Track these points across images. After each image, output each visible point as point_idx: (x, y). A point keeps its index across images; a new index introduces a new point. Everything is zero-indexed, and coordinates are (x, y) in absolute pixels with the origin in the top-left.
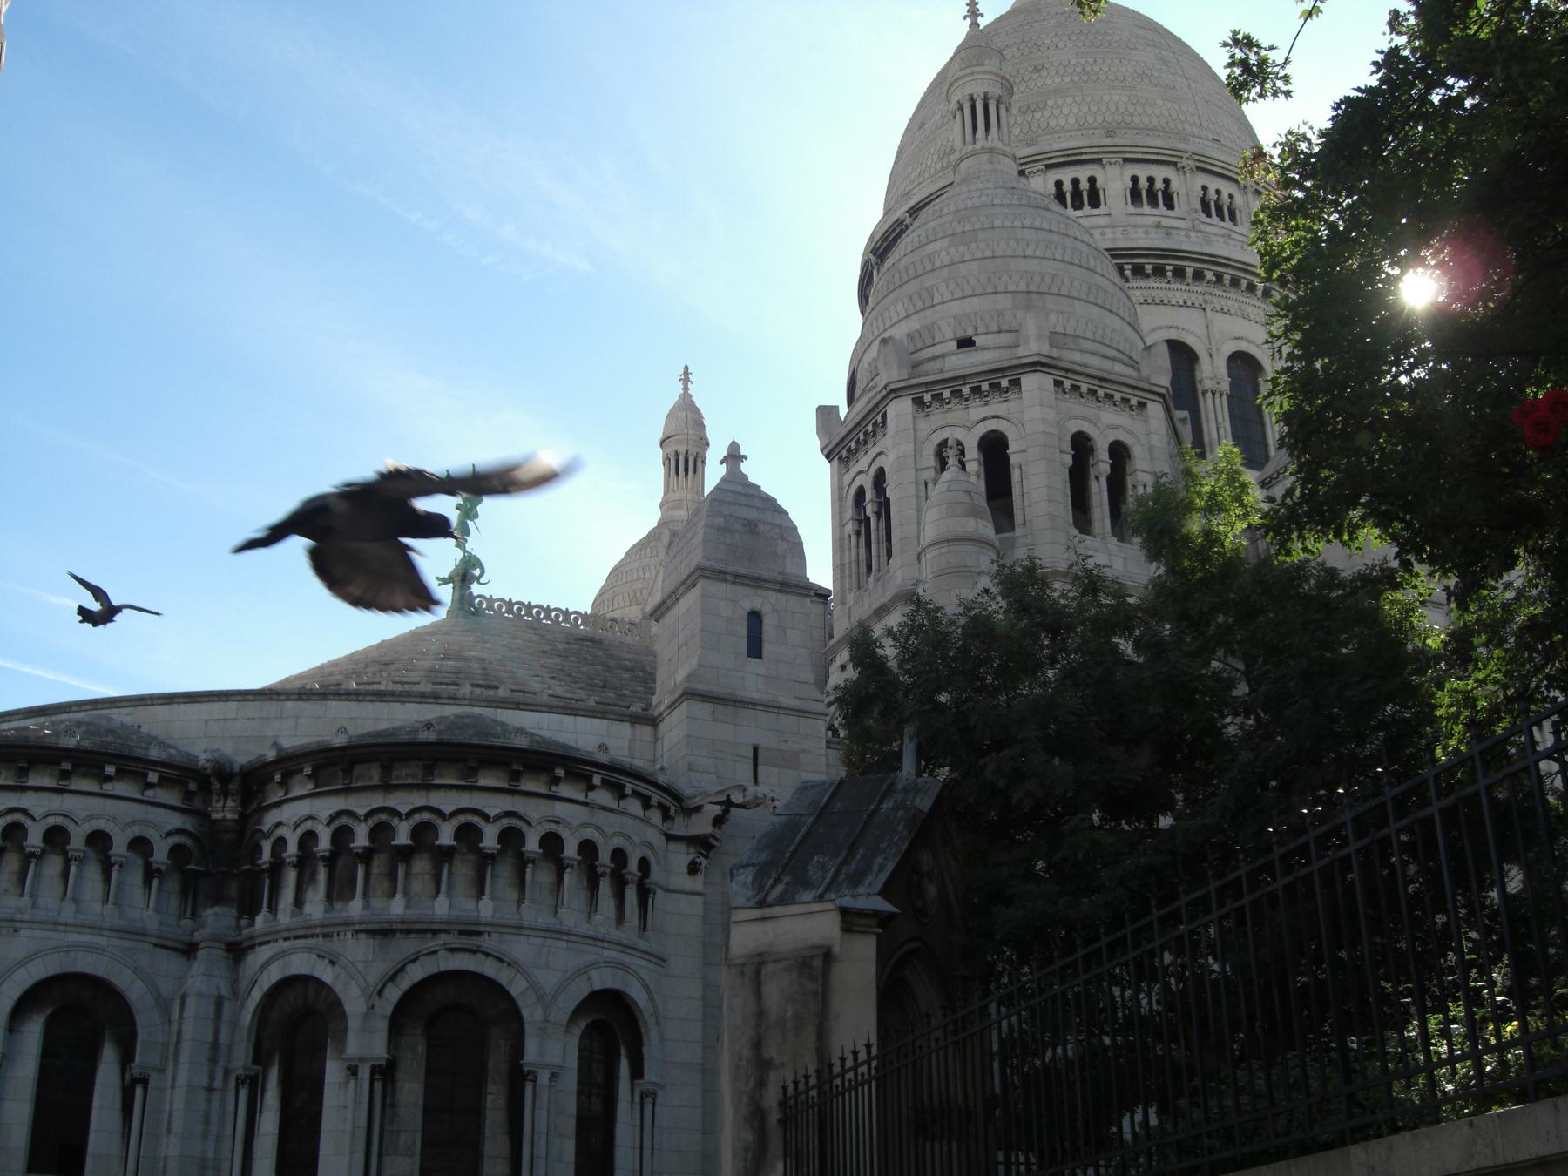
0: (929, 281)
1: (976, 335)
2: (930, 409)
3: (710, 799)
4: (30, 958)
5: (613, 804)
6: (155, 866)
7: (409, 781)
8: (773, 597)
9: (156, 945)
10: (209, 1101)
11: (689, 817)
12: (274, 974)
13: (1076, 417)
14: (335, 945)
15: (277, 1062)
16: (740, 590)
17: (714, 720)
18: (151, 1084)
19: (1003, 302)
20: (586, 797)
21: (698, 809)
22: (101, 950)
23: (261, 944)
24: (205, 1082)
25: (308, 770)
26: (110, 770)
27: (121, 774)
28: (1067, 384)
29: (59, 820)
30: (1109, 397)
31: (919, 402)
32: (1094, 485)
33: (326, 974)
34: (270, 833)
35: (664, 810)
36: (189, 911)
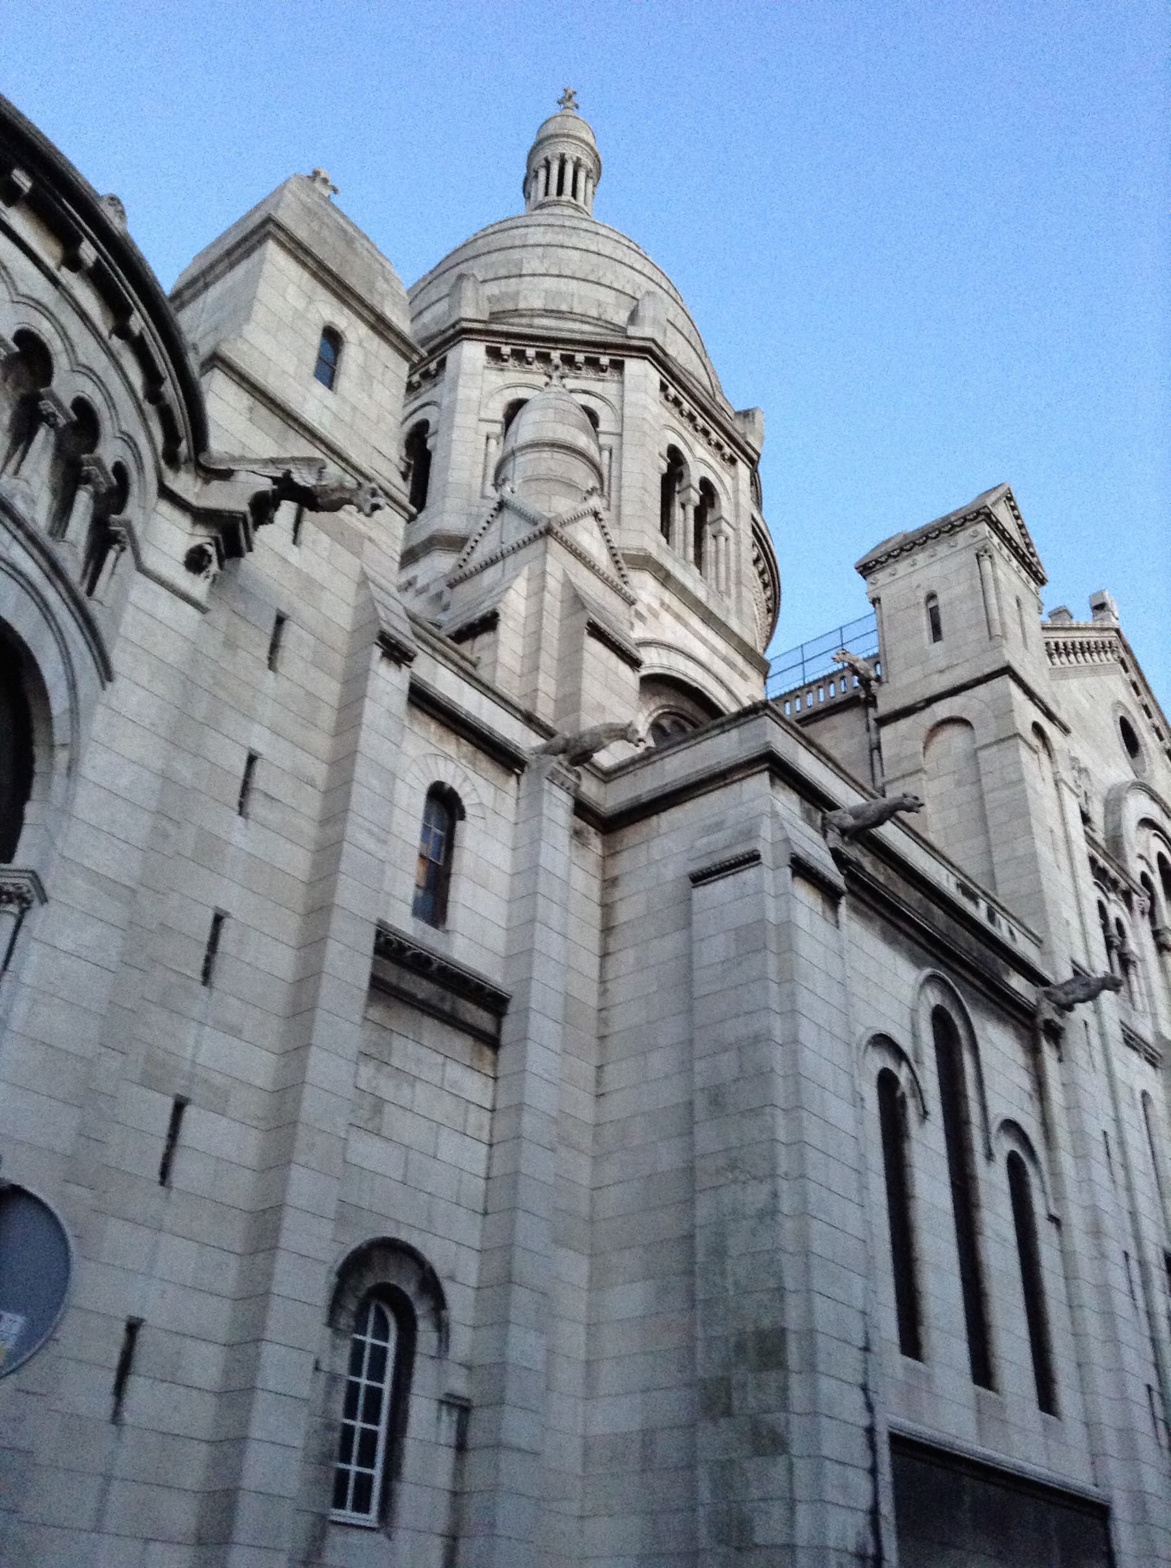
0: (516, 254)
1: (571, 313)
2: (505, 364)
3: (255, 467)
5: (105, 333)
8: (363, 330)
11: (207, 482)
13: (673, 430)
16: (322, 294)
17: (250, 420)
19: (608, 296)
20: (59, 269)
21: (226, 475)
28: (672, 391)
30: (706, 433)
31: (494, 354)
32: (678, 513)
35: (172, 438)
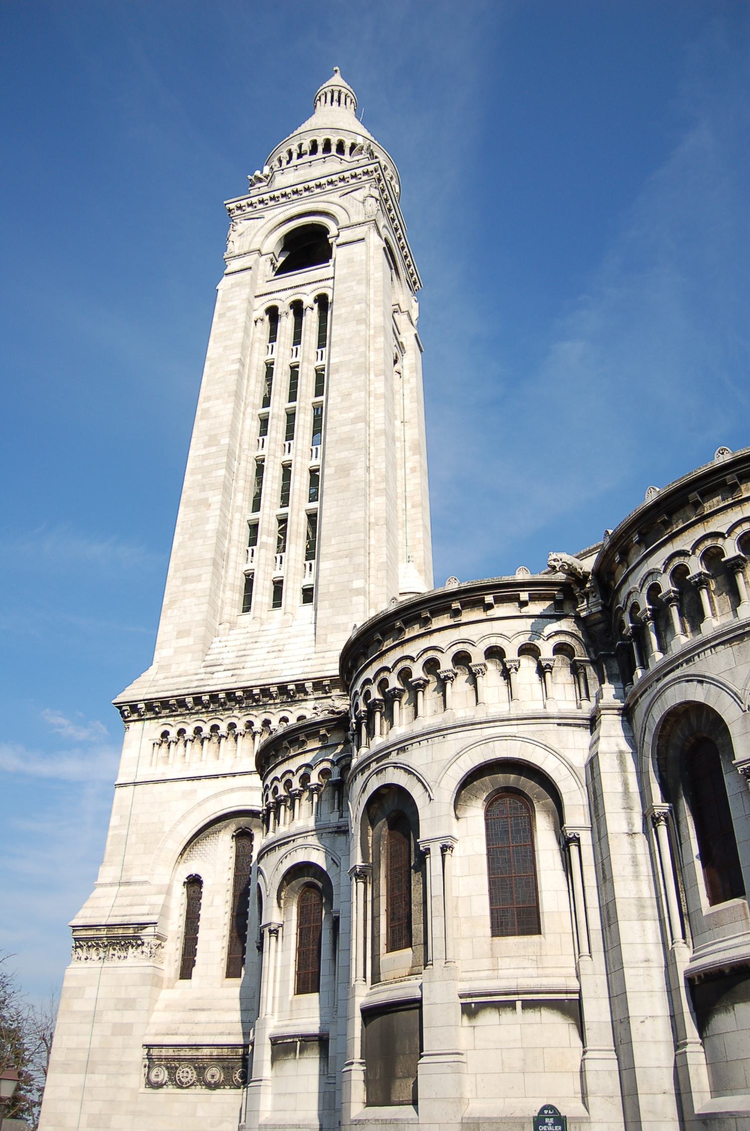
4: (458, 755)
6: (544, 664)
7: (722, 505)
9: (559, 724)
10: (633, 845)
12: (658, 714)
14: (698, 666)
15: (682, 792)
18: (582, 842)
22: (513, 737)
23: (641, 696)
24: (625, 828)
25: (636, 538)
26: (489, 599)
27: (499, 600)
29: (460, 647)
33: (697, 693)
34: (625, 605)
36: (584, 695)
